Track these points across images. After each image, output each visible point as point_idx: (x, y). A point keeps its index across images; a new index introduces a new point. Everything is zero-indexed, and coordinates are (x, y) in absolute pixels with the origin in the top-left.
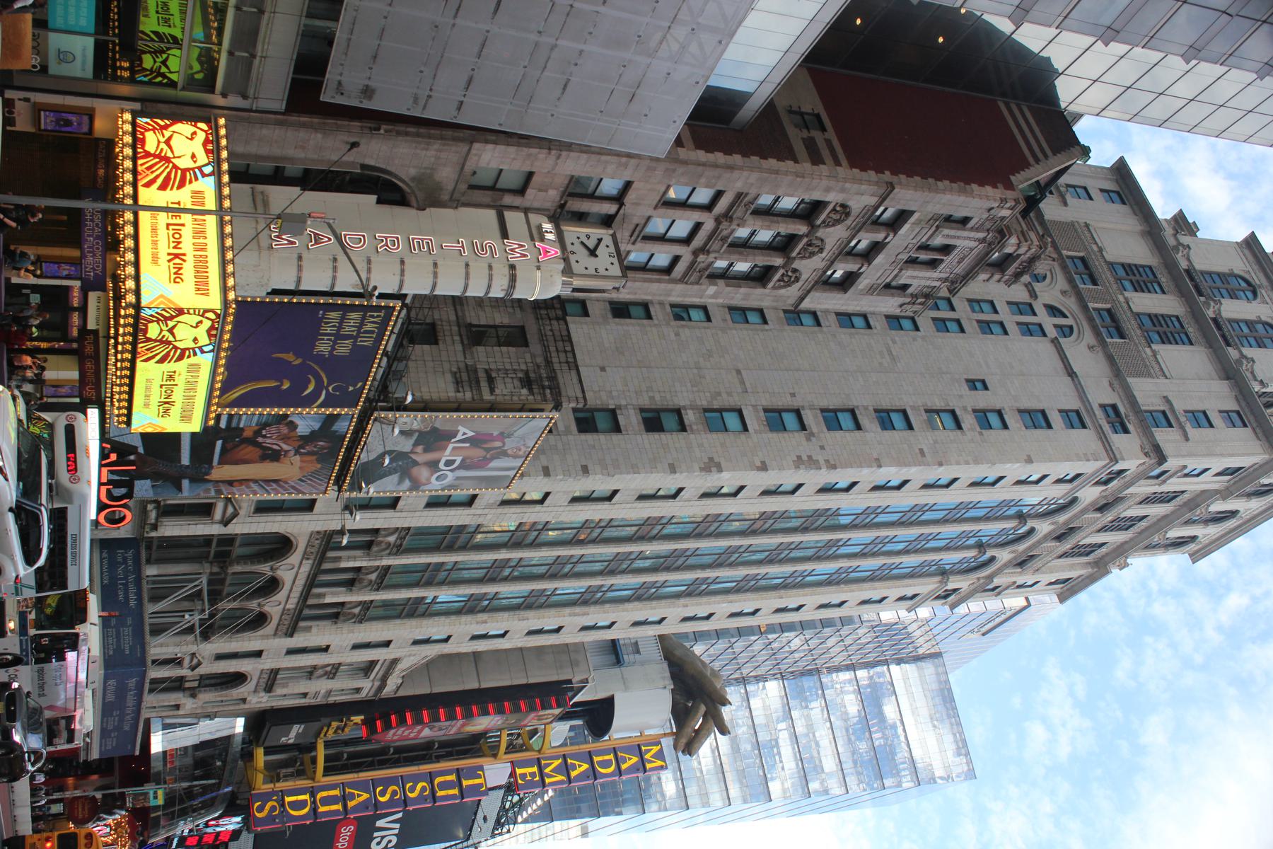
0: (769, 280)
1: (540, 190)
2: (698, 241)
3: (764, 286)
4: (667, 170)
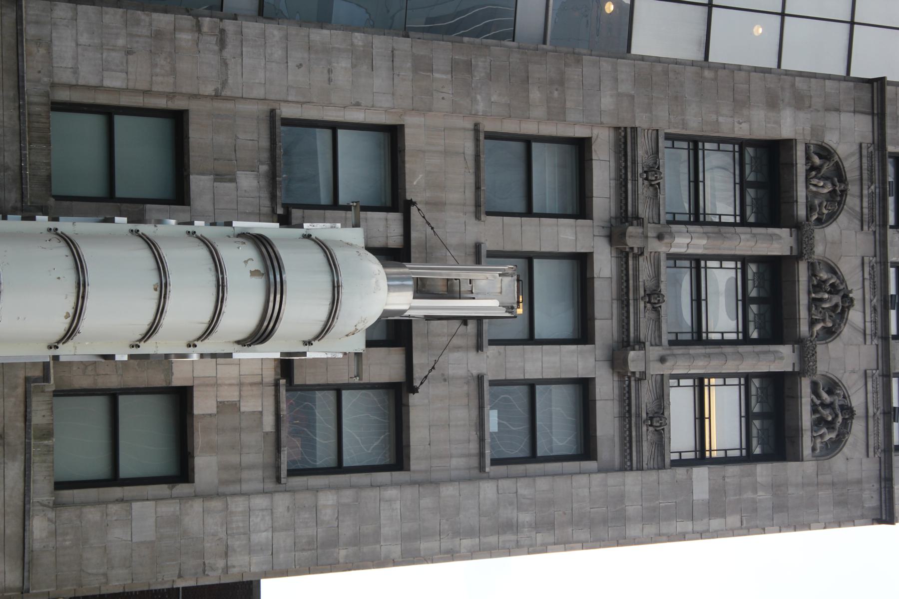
0: (798, 431)
1: (219, 177)
3: (797, 457)
4: (454, 67)
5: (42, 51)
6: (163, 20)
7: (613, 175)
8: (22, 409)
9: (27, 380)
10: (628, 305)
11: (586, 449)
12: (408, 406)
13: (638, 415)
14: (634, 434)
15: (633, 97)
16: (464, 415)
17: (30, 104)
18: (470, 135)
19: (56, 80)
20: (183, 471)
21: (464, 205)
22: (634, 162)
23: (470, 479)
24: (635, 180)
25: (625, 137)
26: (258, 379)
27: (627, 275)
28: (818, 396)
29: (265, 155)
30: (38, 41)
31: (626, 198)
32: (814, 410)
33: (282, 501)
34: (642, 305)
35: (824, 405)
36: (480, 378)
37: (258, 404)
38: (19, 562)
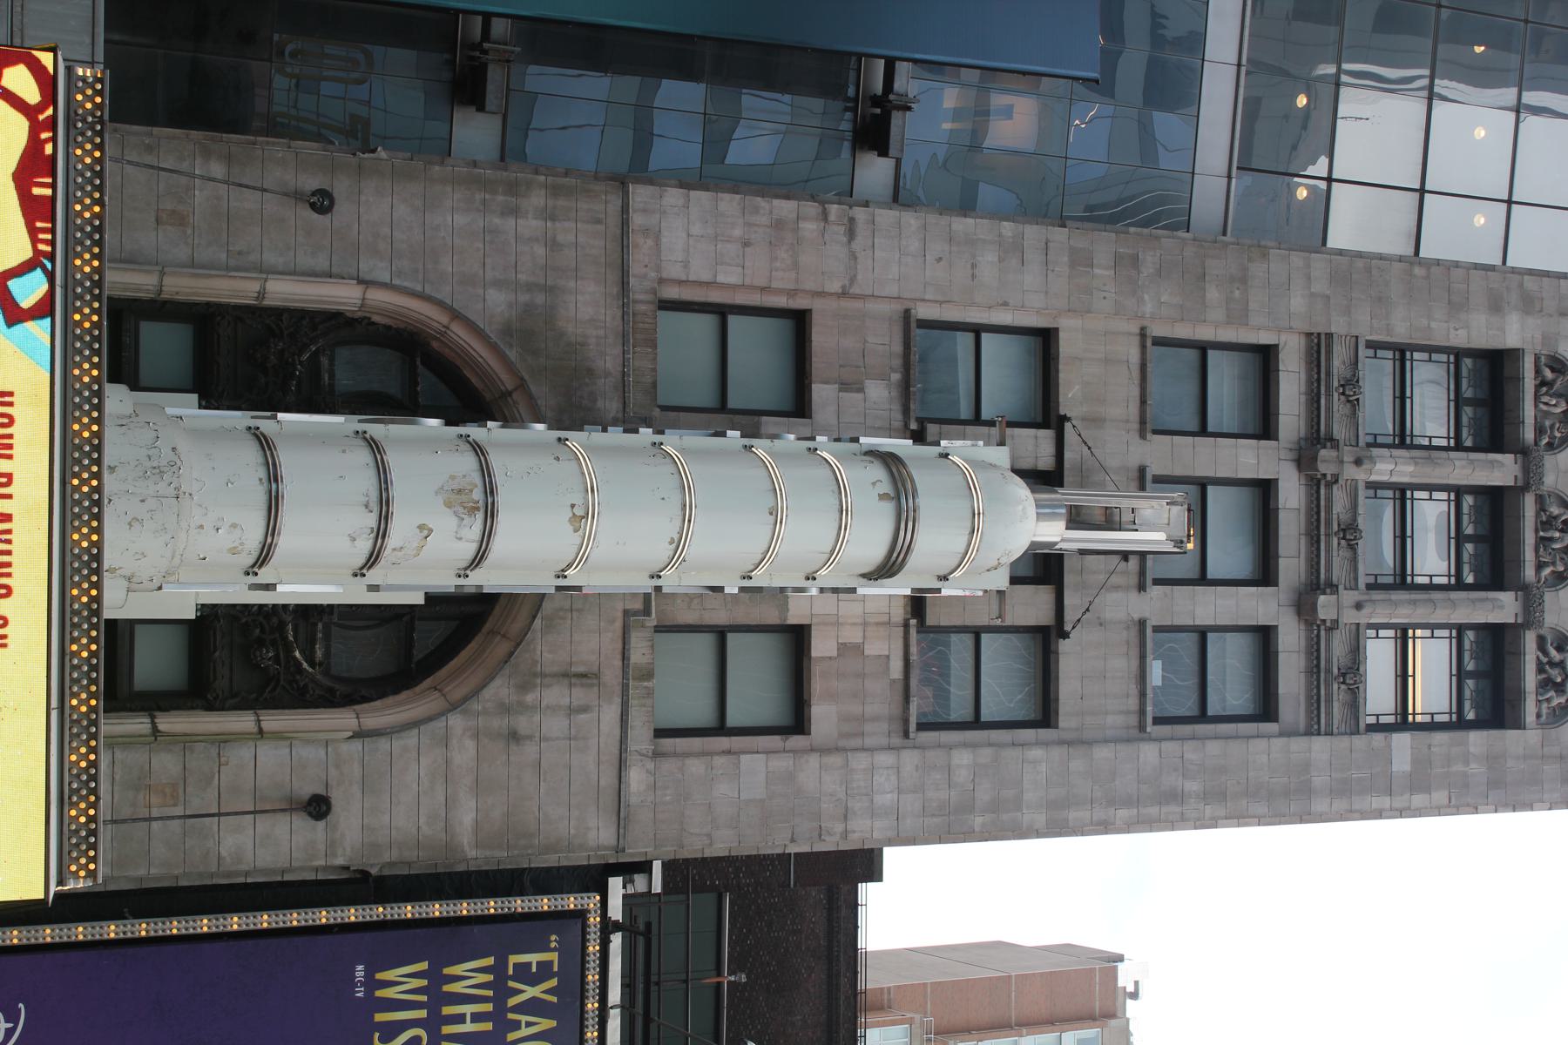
0: (1520, 694)
1: (845, 386)
2: (1291, 565)
3: (1519, 724)
4: (1118, 260)
5: (650, 242)
6: (785, 208)
7: (1303, 389)
8: (620, 646)
9: (626, 613)
10: (1318, 542)
11: (1266, 708)
12: (1057, 653)
13: (1329, 671)
14: (1323, 692)
15: (1328, 297)
16: (1122, 664)
17: (635, 302)
18: (1136, 340)
19: (664, 275)
20: (798, 723)
21: (1127, 421)
22: (1329, 374)
23: (1128, 740)
24: (1329, 395)
25: (1319, 345)
26: (886, 618)
27: (1318, 506)
28: (1545, 653)
29: (897, 362)
30: (646, 232)
31: (1319, 416)
32: (1540, 669)
33: (910, 759)
34: (1335, 541)
35: (1552, 664)
36: (1142, 623)
37: (886, 647)
38: (614, 818)
